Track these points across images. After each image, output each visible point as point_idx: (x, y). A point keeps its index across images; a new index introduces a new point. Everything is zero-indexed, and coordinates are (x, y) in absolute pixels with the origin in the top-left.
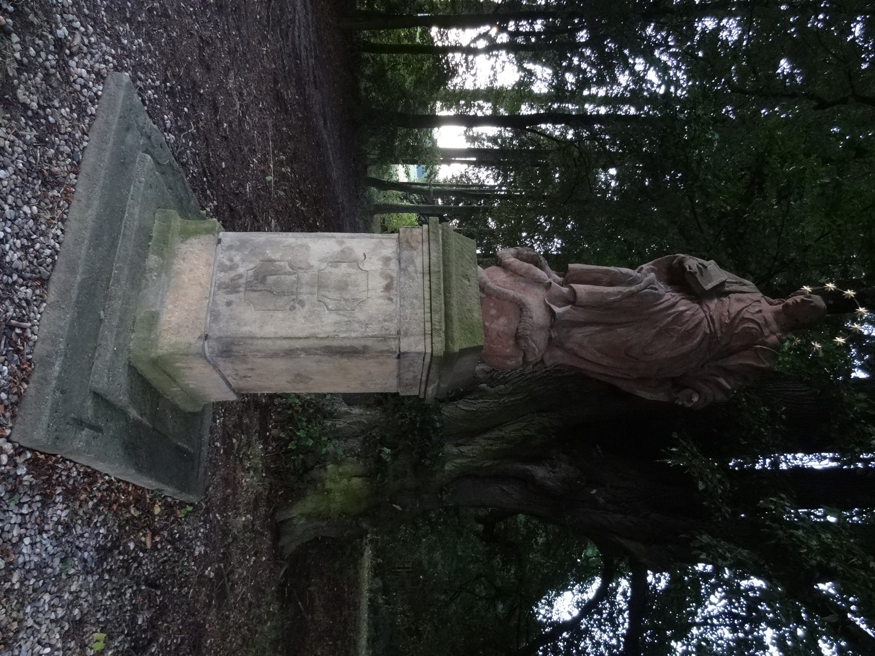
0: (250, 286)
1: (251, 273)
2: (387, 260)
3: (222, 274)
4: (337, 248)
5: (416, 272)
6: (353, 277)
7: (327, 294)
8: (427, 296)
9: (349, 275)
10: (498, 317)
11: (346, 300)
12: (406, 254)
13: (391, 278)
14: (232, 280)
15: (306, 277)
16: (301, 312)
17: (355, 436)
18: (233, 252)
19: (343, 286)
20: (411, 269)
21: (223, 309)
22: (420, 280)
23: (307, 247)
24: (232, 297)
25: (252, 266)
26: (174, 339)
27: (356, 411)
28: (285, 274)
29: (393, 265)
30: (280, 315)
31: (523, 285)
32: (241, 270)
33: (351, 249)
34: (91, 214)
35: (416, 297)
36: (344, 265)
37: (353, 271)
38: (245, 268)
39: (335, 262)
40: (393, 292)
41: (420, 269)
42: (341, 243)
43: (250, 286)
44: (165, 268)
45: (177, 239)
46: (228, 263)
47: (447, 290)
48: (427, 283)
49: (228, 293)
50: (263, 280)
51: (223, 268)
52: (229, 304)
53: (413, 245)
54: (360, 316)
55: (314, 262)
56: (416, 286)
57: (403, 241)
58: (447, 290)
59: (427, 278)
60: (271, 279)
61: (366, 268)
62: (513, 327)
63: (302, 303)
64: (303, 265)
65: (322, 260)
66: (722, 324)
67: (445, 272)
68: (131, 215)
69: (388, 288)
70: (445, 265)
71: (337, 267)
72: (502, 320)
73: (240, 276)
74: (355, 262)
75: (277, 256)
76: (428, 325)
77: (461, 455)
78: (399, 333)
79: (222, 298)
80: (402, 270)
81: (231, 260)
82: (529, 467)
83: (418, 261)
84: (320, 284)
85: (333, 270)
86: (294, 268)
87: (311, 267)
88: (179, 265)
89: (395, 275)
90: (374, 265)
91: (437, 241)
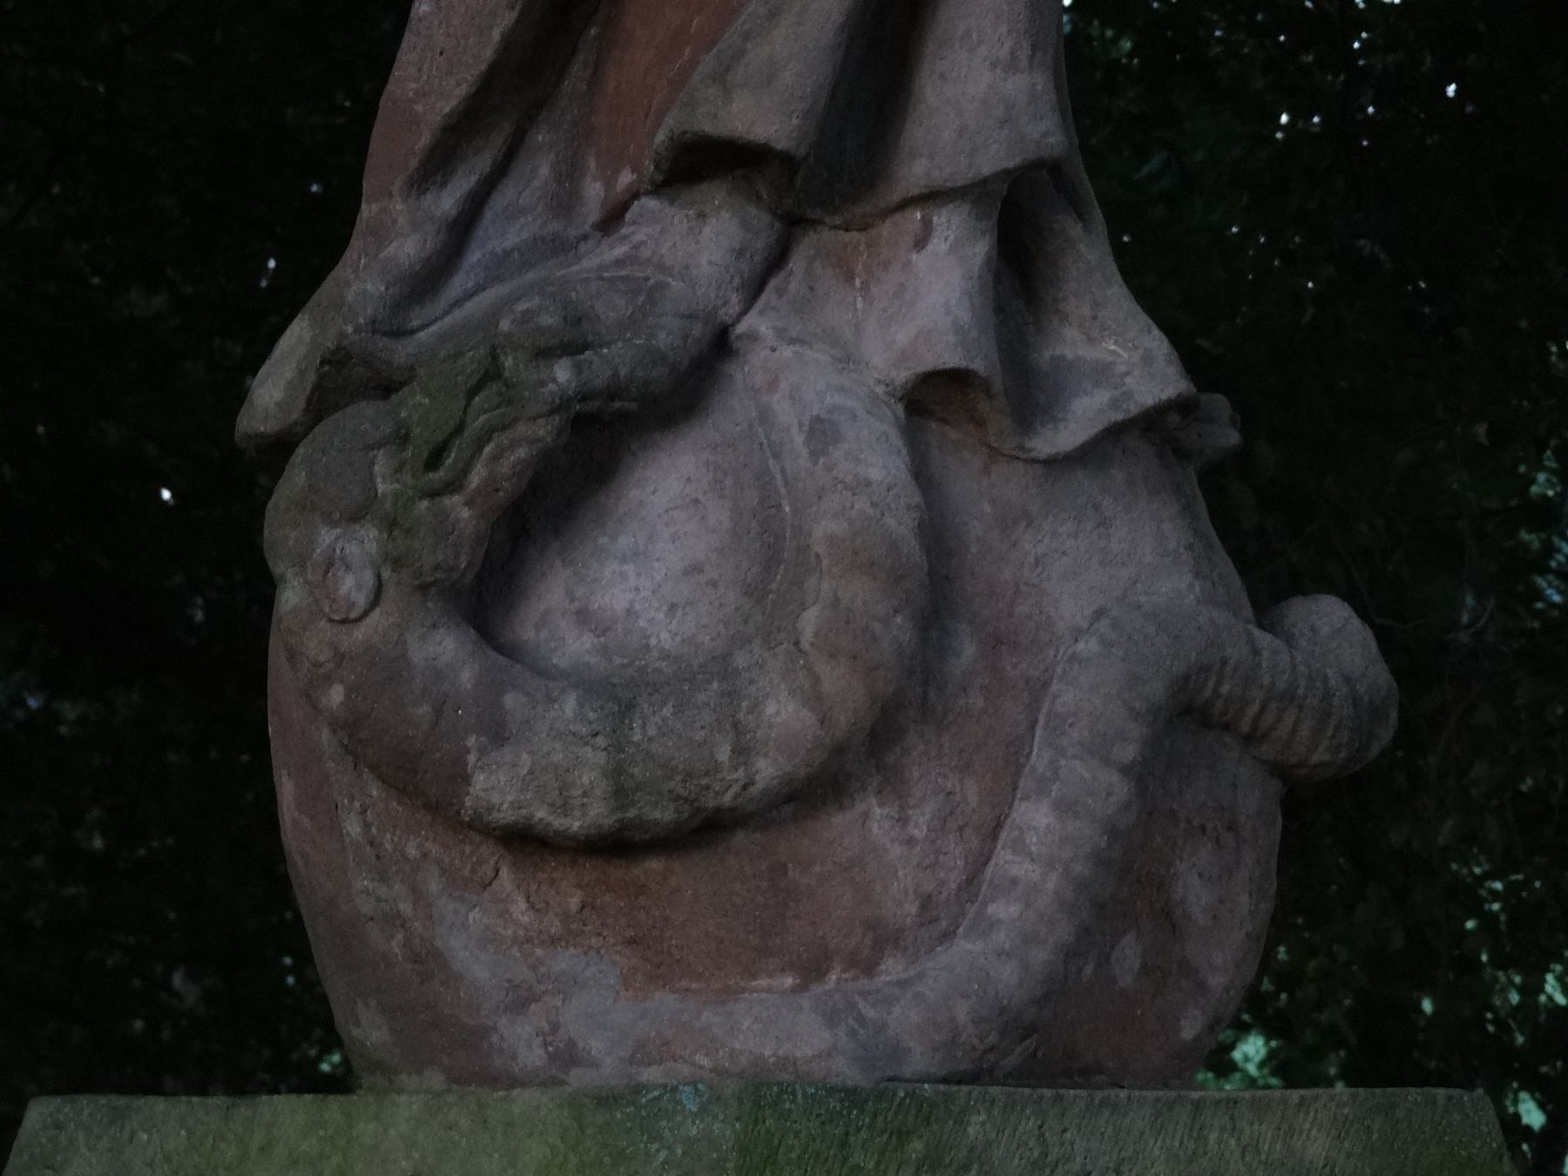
10: (1170, 920)
31: (968, 649)
72: (1194, 891)
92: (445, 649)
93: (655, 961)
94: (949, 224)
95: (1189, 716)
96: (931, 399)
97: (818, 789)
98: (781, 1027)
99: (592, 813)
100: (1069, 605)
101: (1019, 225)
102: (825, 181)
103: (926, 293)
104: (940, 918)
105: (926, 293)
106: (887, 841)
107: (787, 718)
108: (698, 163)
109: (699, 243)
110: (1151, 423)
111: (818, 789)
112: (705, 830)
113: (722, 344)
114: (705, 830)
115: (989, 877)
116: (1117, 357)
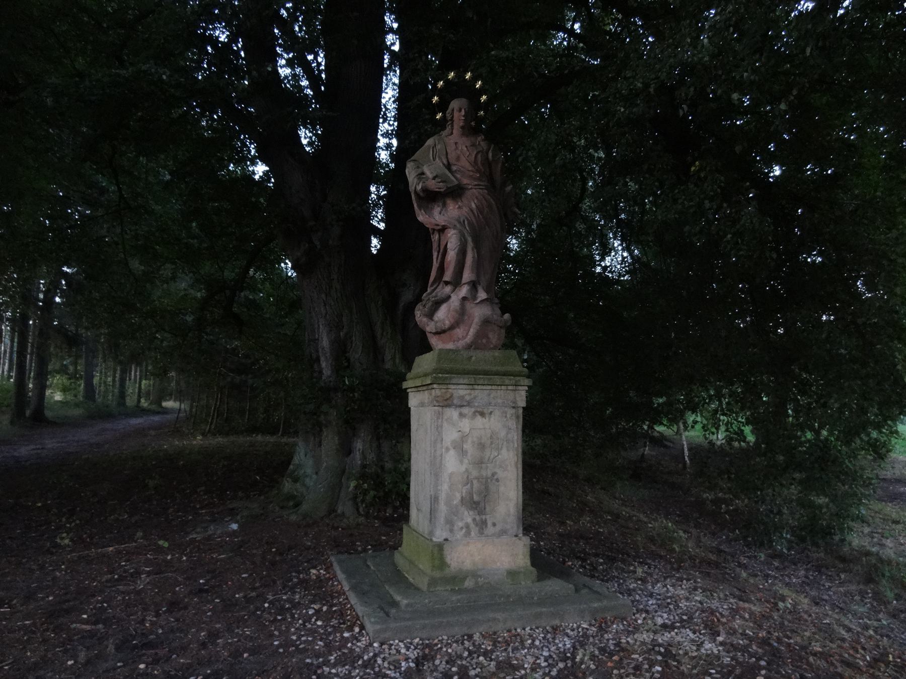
0: (481, 512)
1: (471, 513)
2: (462, 415)
3: (473, 534)
4: (452, 452)
5: (470, 394)
6: (475, 439)
7: (487, 457)
8: (490, 387)
9: (473, 442)
10: (488, 338)
11: (492, 443)
12: (455, 402)
13: (475, 412)
14: (477, 525)
15: (475, 473)
16: (501, 474)
17: (379, 447)
18: (456, 528)
19: (482, 446)
20: (467, 398)
21: (498, 528)
22: (477, 392)
23: (451, 474)
24: (489, 523)
25: (466, 513)
26: (521, 557)
27: (359, 445)
28: (472, 488)
29: (465, 410)
30: (502, 489)
31: (466, 318)
32: (469, 520)
33: (454, 442)
34: (499, 616)
35: (489, 395)
36: (465, 446)
37: (470, 441)
38: (468, 517)
39: (462, 453)
40: (485, 411)
41: (468, 391)
42: (448, 449)
43: (481, 512)
44: (474, 574)
45: (447, 571)
46: (464, 531)
47: (486, 373)
48: (480, 387)
49: (486, 526)
50: (477, 503)
51: (468, 533)
52: (494, 525)
53: (449, 396)
54: (503, 434)
55: (463, 469)
56: (481, 395)
57: (446, 403)
58: (486, 373)
59: (476, 387)
60: (476, 498)
61: (467, 430)
62: (496, 328)
63: (493, 474)
64: (465, 477)
65: (461, 462)
66: (479, 179)
67: (473, 374)
68: (459, 601)
69: (482, 414)
70: (468, 373)
71: (467, 452)
72: (491, 336)
73: (474, 520)
74: (464, 438)
75: (458, 496)
76: (510, 388)
77: (393, 358)
78: (514, 407)
79: (490, 530)
80: (469, 404)
81: (462, 528)
82: (402, 305)
83: (462, 392)
84: (480, 463)
85: (469, 454)
86: (468, 481)
87: (467, 470)
88: (468, 565)
89: (473, 410)
90: (465, 425)
91: (451, 378)
92: (425, 319)
93: (444, 342)
94: (466, 286)
95: (486, 322)
96: (464, 299)
97: (452, 328)
98: (450, 346)
99: (434, 331)
100: (476, 314)
101: (474, 285)
102: (456, 283)
103: (464, 291)
104: (464, 338)
105: (464, 291)
106: (459, 332)
107: (447, 323)
108: (447, 283)
109: (448, 289)
110: (486, 300)
111: (452, 328)
112: (444, 332)
113: (449, 297)
114: (444, 332)
115: (467, 334)
116: (482, 295)
